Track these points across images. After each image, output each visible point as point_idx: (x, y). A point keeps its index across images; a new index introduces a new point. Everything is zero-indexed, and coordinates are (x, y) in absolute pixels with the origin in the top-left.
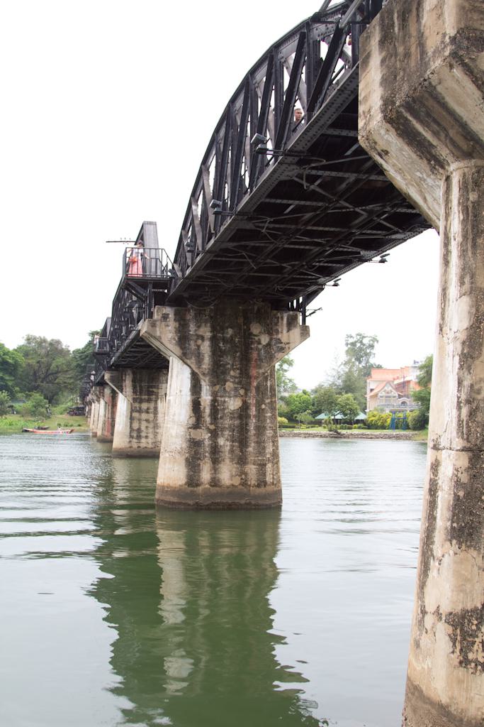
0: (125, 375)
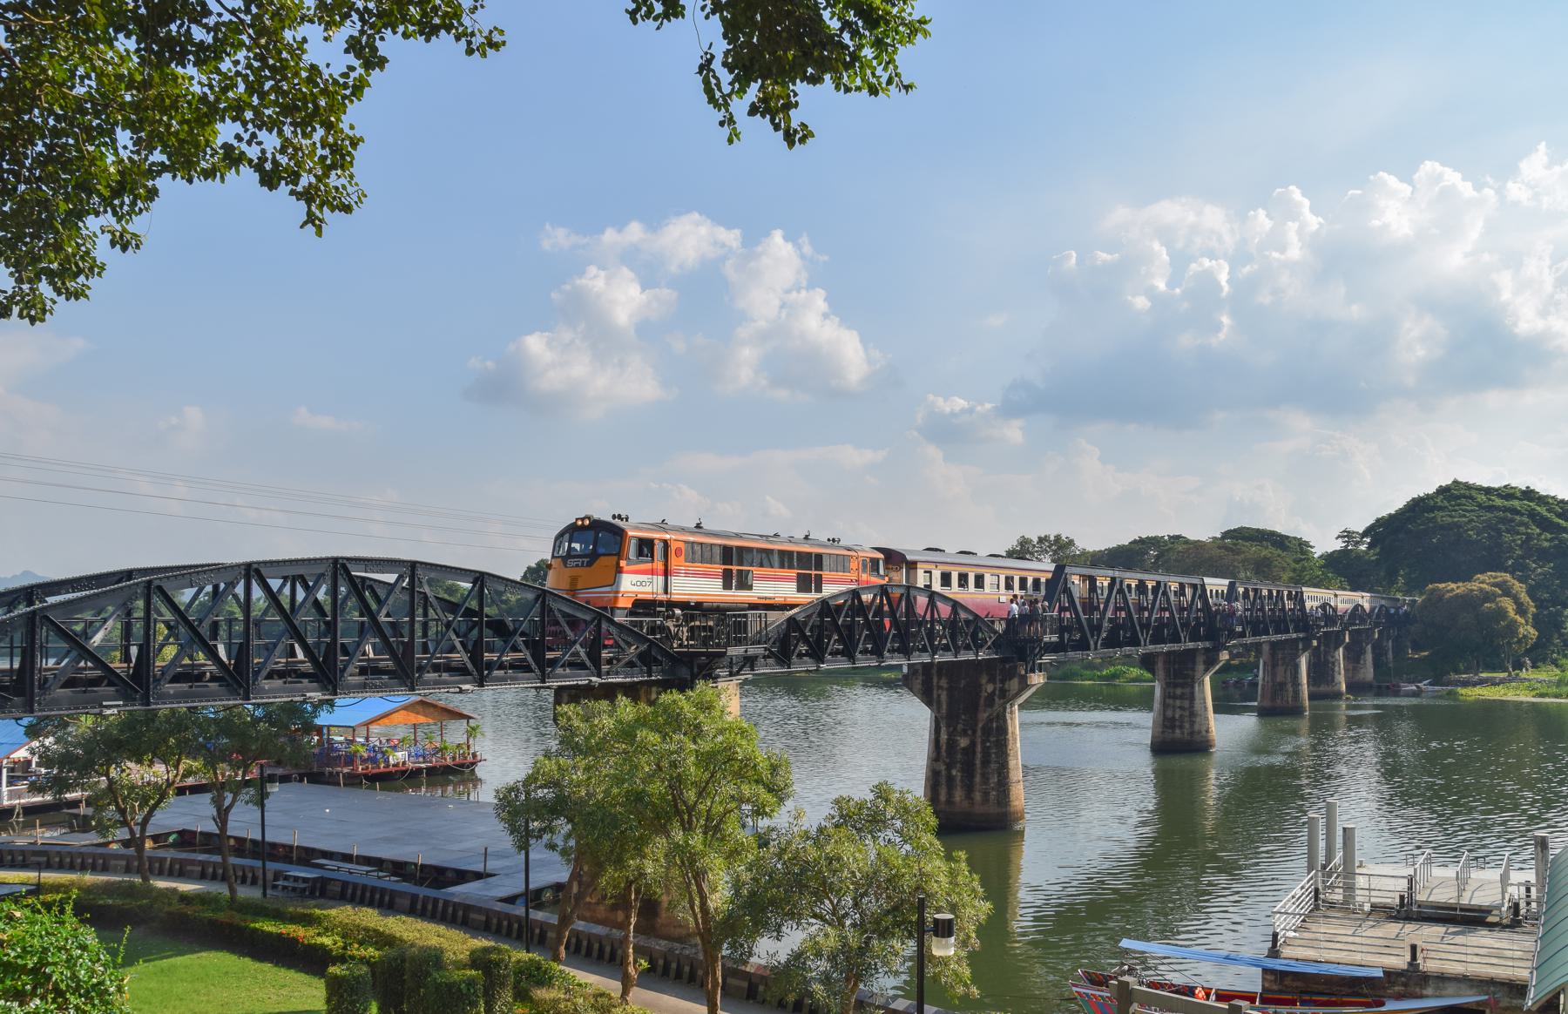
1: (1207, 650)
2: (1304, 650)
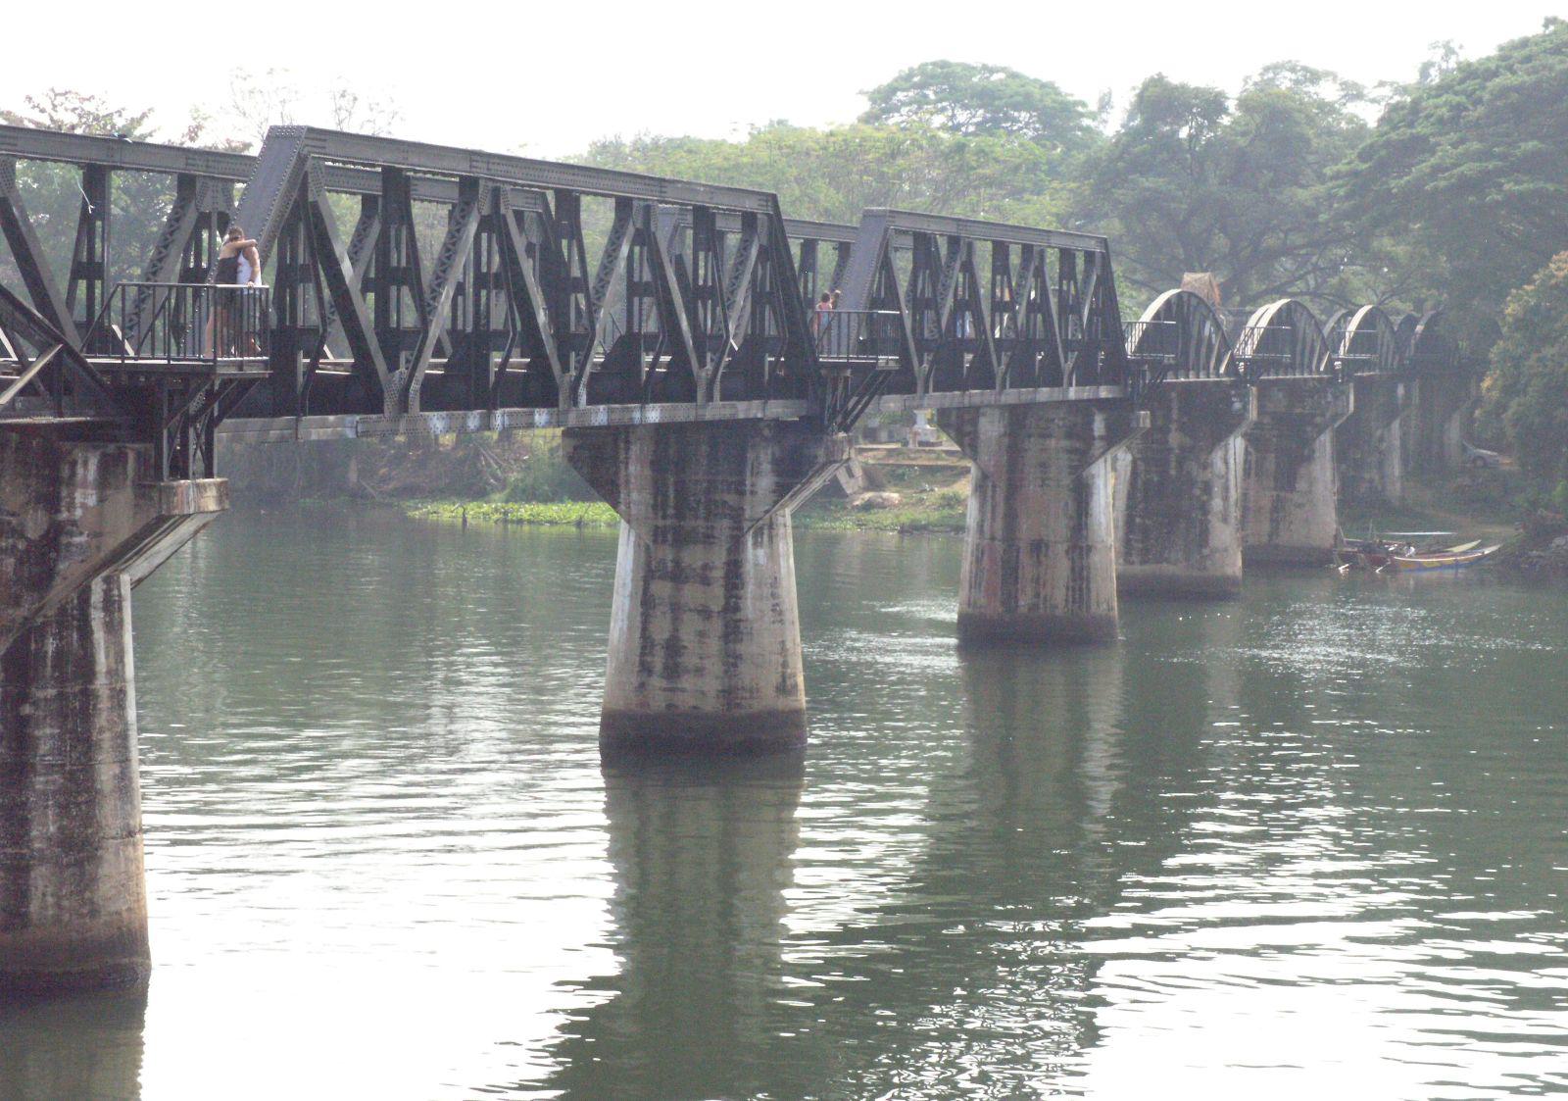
0: (627, 442)
1: (780, 426)
2: (1112, 439)
